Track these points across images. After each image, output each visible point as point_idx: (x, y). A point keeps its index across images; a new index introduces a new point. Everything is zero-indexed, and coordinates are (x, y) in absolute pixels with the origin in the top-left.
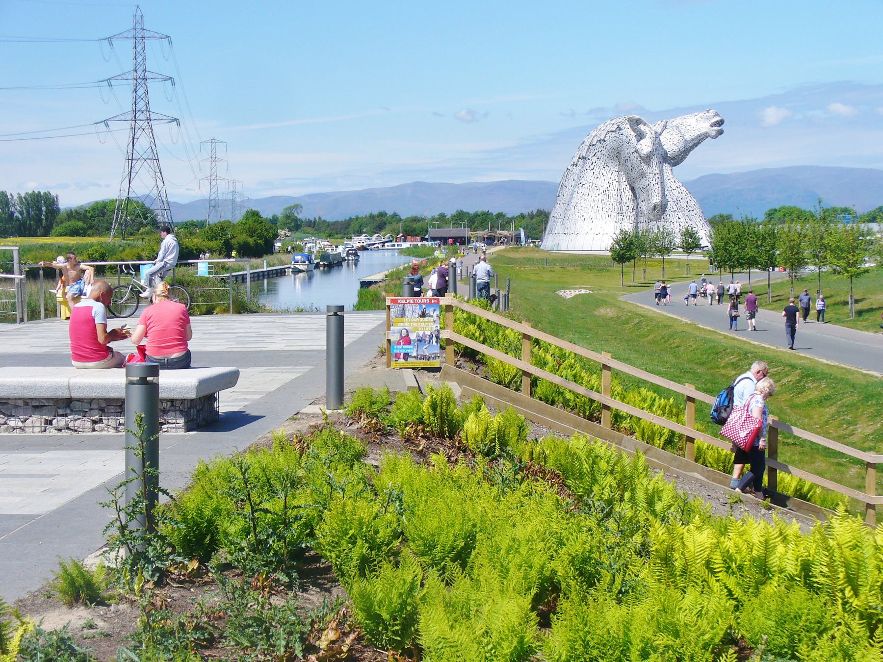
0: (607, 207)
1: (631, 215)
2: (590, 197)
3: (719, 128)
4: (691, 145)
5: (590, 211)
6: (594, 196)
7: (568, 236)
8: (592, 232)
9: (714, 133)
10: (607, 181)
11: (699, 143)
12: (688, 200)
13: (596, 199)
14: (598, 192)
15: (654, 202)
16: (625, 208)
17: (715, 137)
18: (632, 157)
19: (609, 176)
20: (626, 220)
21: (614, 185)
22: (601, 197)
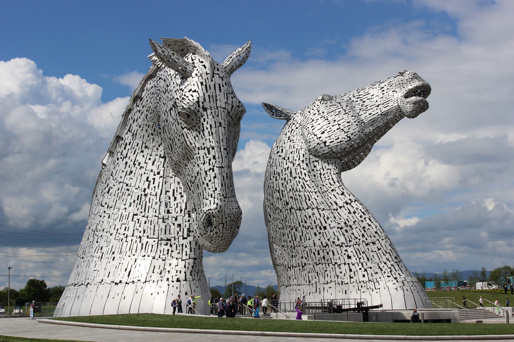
0: (141, 229)
1: (185, 242)
2: (116, 210)
4: (371, 129)
5: (113, 236)
8: (111, 278)
12: (364, 224)
13: (125, 213)
14: (129, 200)
15: (205, 209)
16: (174, 229)
17: (413, 115)
19: (150, 166)
20: (175, 254)
21: (156, 184)
22: (132, 210)
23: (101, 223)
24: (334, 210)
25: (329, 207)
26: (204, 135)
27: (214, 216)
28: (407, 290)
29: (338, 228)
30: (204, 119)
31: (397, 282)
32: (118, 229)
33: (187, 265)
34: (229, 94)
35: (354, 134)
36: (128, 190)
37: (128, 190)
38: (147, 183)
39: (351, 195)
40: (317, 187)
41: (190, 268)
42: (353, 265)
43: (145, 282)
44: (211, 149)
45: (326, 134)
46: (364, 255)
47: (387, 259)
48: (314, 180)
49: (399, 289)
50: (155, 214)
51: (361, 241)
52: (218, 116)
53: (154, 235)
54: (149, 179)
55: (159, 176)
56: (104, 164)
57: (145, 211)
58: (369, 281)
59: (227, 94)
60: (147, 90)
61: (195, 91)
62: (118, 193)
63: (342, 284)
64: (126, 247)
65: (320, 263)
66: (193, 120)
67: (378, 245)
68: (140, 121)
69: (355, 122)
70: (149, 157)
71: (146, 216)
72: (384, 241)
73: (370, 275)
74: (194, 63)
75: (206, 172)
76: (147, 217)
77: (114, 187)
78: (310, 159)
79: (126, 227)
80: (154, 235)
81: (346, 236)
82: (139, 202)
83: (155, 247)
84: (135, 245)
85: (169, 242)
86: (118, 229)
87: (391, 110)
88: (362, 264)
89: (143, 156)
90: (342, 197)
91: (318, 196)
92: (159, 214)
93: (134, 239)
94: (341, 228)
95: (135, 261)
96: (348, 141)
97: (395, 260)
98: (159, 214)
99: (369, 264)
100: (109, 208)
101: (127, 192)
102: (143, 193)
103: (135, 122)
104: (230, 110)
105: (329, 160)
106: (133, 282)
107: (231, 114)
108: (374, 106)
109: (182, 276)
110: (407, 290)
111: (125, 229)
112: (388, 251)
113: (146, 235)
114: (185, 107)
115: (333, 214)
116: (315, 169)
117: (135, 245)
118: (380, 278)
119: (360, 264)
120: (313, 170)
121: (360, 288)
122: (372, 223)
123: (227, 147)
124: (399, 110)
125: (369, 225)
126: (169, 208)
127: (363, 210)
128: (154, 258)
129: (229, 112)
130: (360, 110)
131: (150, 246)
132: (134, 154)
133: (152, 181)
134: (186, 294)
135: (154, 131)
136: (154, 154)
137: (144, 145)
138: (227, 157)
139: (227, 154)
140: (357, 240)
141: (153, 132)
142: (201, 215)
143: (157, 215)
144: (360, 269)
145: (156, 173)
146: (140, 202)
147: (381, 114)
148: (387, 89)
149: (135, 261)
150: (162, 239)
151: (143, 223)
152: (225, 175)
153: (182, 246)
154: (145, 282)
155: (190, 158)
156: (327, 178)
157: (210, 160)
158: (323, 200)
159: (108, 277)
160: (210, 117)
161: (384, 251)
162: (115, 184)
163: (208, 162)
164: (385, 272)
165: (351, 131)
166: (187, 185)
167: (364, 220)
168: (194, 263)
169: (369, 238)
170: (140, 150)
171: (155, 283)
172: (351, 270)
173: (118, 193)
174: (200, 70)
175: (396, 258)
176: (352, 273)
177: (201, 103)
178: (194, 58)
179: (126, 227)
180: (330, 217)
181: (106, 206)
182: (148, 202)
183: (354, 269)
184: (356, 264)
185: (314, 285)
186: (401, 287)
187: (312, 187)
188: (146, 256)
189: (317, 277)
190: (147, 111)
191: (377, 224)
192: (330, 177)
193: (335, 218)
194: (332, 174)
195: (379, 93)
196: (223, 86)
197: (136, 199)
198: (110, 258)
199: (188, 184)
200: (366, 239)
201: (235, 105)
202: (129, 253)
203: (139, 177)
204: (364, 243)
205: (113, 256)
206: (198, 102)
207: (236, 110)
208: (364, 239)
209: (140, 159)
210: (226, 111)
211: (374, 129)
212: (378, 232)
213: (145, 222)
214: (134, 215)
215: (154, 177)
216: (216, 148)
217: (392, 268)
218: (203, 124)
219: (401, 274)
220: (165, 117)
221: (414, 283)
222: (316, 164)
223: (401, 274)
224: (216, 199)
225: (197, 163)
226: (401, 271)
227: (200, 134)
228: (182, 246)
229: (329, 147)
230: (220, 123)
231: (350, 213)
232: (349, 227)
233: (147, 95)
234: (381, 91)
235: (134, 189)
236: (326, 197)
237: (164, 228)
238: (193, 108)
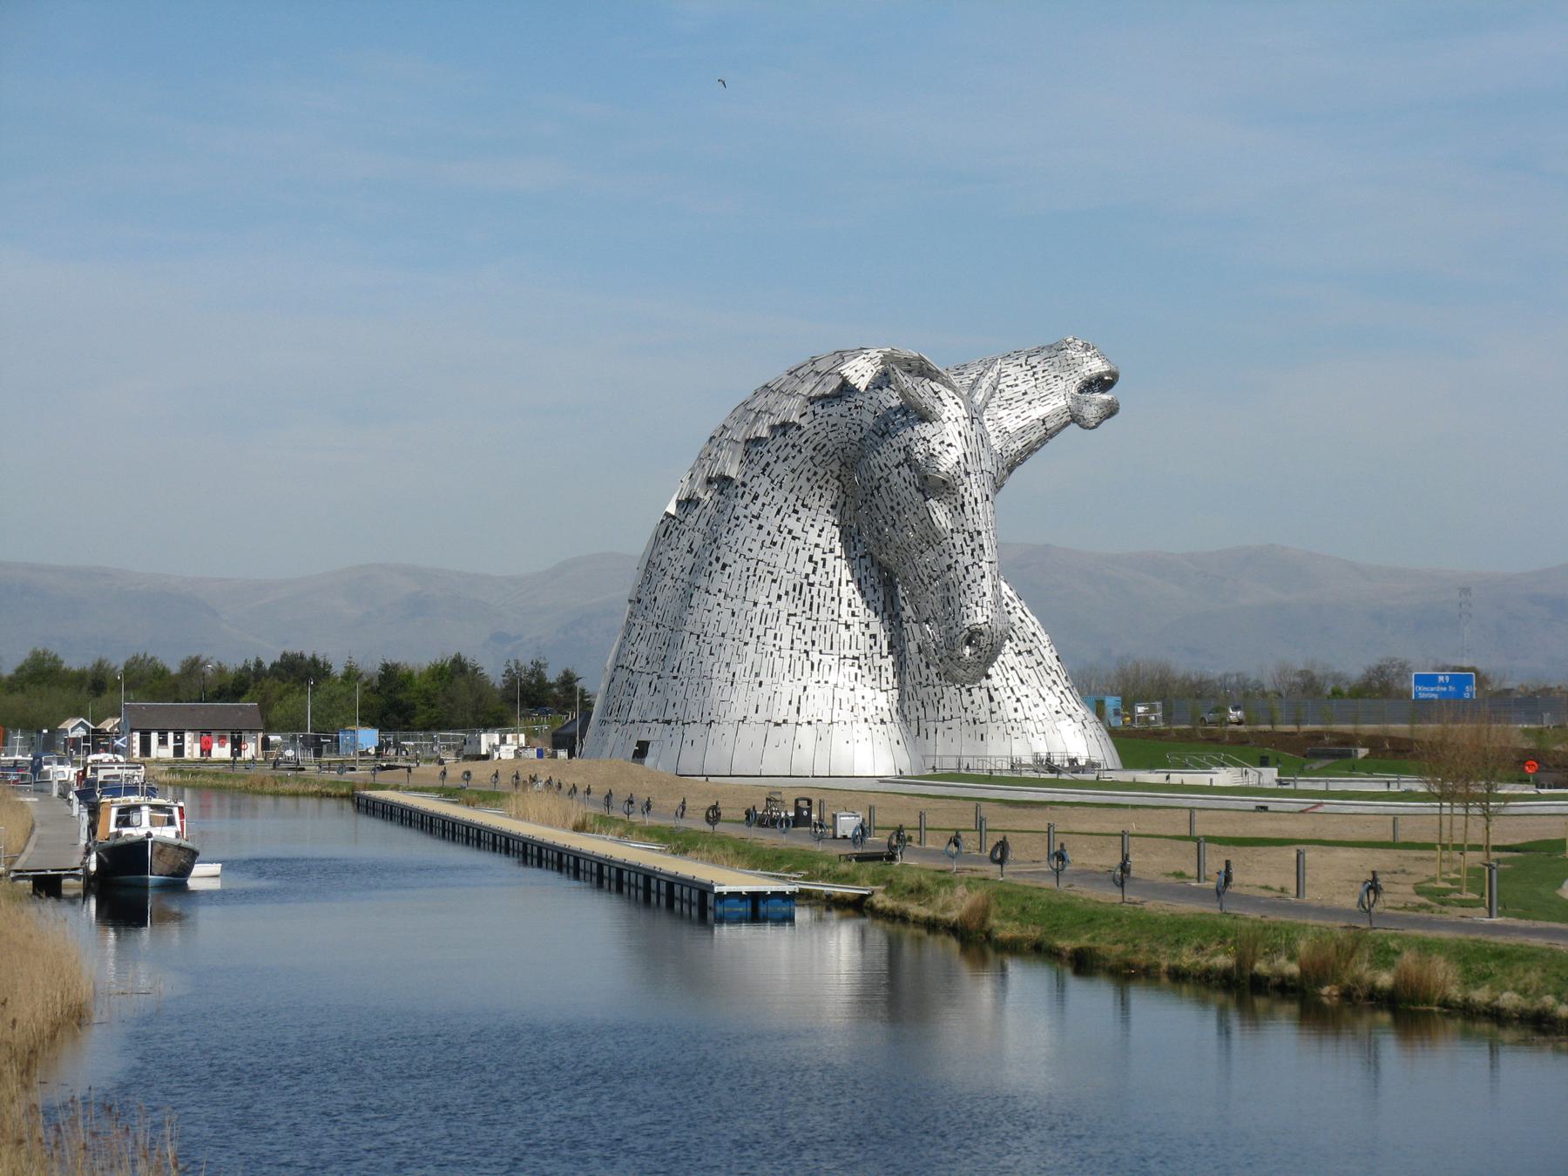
3: (1106, 397)
4: (1020, 444)
6: (762, 600)
7: (679, 728)
8: (763, 716)
9: (1090, 413)
10: (804, 555)
11: (1042, 441)
15: (967, 623)
18: (894, 478)
19: (812, 537)
20: (868, 679)
21: (829, 567)
23: (713, 621)
26: (963, 512)
27: (981, 634)
30: (966, 489)
32: (758, 637)
33: (890, 698)
36: (772, 573)
37: (772, 573)
38: (809, 567)
41: (895, 704)
42: (996, 690)
43: (832, 723)
44: (975, 534)
47: (1054, 682)
49: (1078, 734)
50: (833, 617)
53: (831, 648)
54: (814, 559)
55: (832, 555)
56: (668, 515)
57: (811, 609)
58: (1026, 719)
60: (815, 415)
61: (950, 445)
62: (748, 577)
63: (975, 723)
64: (781, 665)
65: (928, 685)
66: (948, 489)
68: (795, 464)
70: (810, 522)
71: (814, 618)
73: (1026, 709)
74: (939, 398)
75: (966, 568)
76: (817, 620)
77: (734, 565)
79: (776, 634)
80: (831, 648)
82: (797, 596)
83: (835, 668)
84: (799, 664)
85: (856, 661)
86: (758, 637)
87: (1055, 412)
88: (1012, 689)
89: (798, 519)
92: (839, 616)
93: (795, 654)
95: (805, 688)
97: (1067, 684)
98: (839, 616)
99: (1024, 690)
100: (729, 599)
101: (770, 578)
102: (805, 581)
103: (780, 462)
106: (809, 723)
108: (1023, 402)
109: (887, 718)
111: (775, 638)
112: (1054, 668)
113: (816, 648)
114: (941, 469)
117: (799, 664)
119: (1008, 690)
121: (1010, 731)
124: (1069, 413)
125: (1022, 621)
126: (853, 608)
128: (836, 686)
130: (999, 406)
131: (827, 668)
132: (778, 512)
133: (821, 563)
134: (898, 743)
135: (827, 482)
136: (820, 518)
137: (800, 502)
141: (822, 483)
142: (957, 631)
143: (836, 618)
144: (1009, 698)
145: (827, 550)
146: (800, 593)
148: (1044, 371)
149: (805, 688)
150: (845, 657)
151: (809, 630)
152: (995, 573)
153: (880, 670)
154: (832, 723)
155: (932, 543)
157: (973, 550)
159: (757, 712)
160: (975, 486)
162: (738, 559)
163: (970, 552)
166: (918, 580)
167: (1012, 611)
169: (1021, 644)
170: (791, 508)
171: (849, 725)
172: (991, 699)
173: (748, 577)
174: (953, 412)
176: (994, 704)
177: (961, 465)
178: (937, 390)
179: (776, 634)
181: (723, 594)
182: (816, 597)
183: (996, 699)
184: (1001, 690)
185: (915, 724)
188: (822, 682)
189: (921, 710)
190: (814, 449)
191: (1034, 619)
195: (1028, 378)
197: (790, 589)
198: (752, 682)
199: (922, 580)
200: (1016, 645)
202: (789, 677)
203: (793, 554)
205: (758, 680)
206: (958, 463)
209: (791, 522)
212: (1038, 633)
213: (814, 629)
214: (789, 615)
215: (824, 556)
216: (983, 533)
217: (1062, 697)
218: (963, 497)
220: (884, 475)
224: (984, 609)
225: (947, 551)
227: (956, 509)
228: (880, 670)
230: (987, 496)
233: (816, 423)
234: (1031, 373)
235: (783, 572)
237: (848, 640)
238: (952, 472)
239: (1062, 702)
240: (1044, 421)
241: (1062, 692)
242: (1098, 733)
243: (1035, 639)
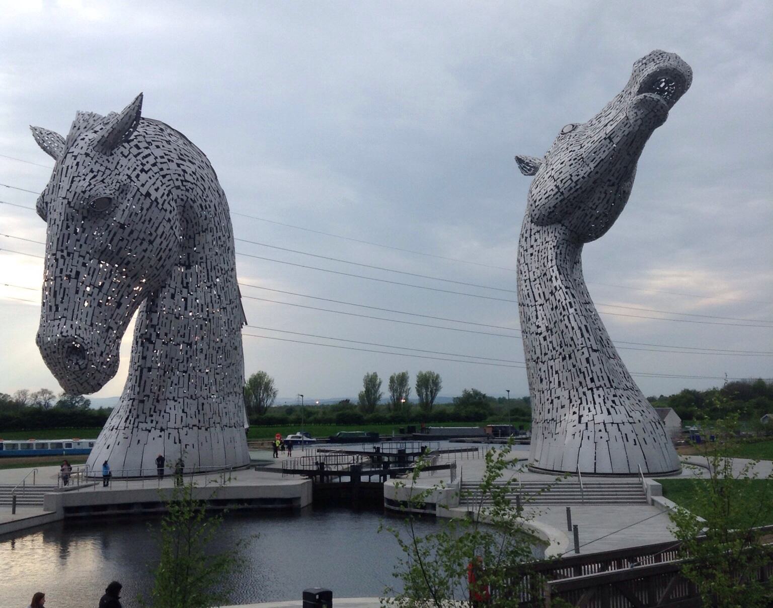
4: (592, 165)
12: (562, 327)
24: (540, 305)
25: (536, 301)
28: (588, 438)
29: (537, 334)
31: (580, 422)
34: (78, 176)
35: (564, 181)
39: (559, 281)
40: (529, 271)
41: (128, 413)
45: (538, 189)
46: (556, 376)
48: (528, 261)
51: (558, 353)
52: (55, 211)
59: (73, 177)
67: (573, 360)
69: (570, 160)
72: (580, 352)
73: (555, 410)
78: (531, 229)
81: (542, 347)
87: (618, 127)
90: (549, 283)
91: (526, 286)
94: (541, 334)
96: (557, 193)
97: (590, 385)
99: (559, 392)
104: (70, 200)
105: (549, 227)
107: (72, 205)
110: (589, 437)
112: (584, 369)
115: (537, 312)
116: (535, 244)
118: (565, 415)
120: (532, 246)
122: (570, 323)
123: (57, 250)
125: (567, 327)
127: (564, 304)
129: (69, 203)
138: (55, 265)
139: (57, 260)
140: (554, 352)
147: (605, 139)
156: (543, 256)
158: (530, 291)
161: (578, 370)
164: (573, 405)
165: (562, 176)
168: (132, 405)
175: (592, 380)
180: (531, 318)
183: (542, 402)
184: (545, 392)
186: (582, 432)
187: (523, 273)
192: (546, 255)
193: (537, 318)
194: (549, 248)
196: (72, 167)
200: (563, 350)
201: (79, 191)
204: (561, 357)
207: (80, 197)
208: (561, 350)
210: (66, 202)
211: (596, 166)
212: (575, 338)
219: (592, 409)
221: (609, 427)
222: (537, 236)
223: (592, 409)
226: (595, 403)
229: (539, 207)
231: (552, 309)
232: (550, 331)
236: (536, 286)
238: (39, 206)
239: (581, 403)
240: (609, 137)
241: (584, 394)
242: (599, 434)
243: (572, 343)
